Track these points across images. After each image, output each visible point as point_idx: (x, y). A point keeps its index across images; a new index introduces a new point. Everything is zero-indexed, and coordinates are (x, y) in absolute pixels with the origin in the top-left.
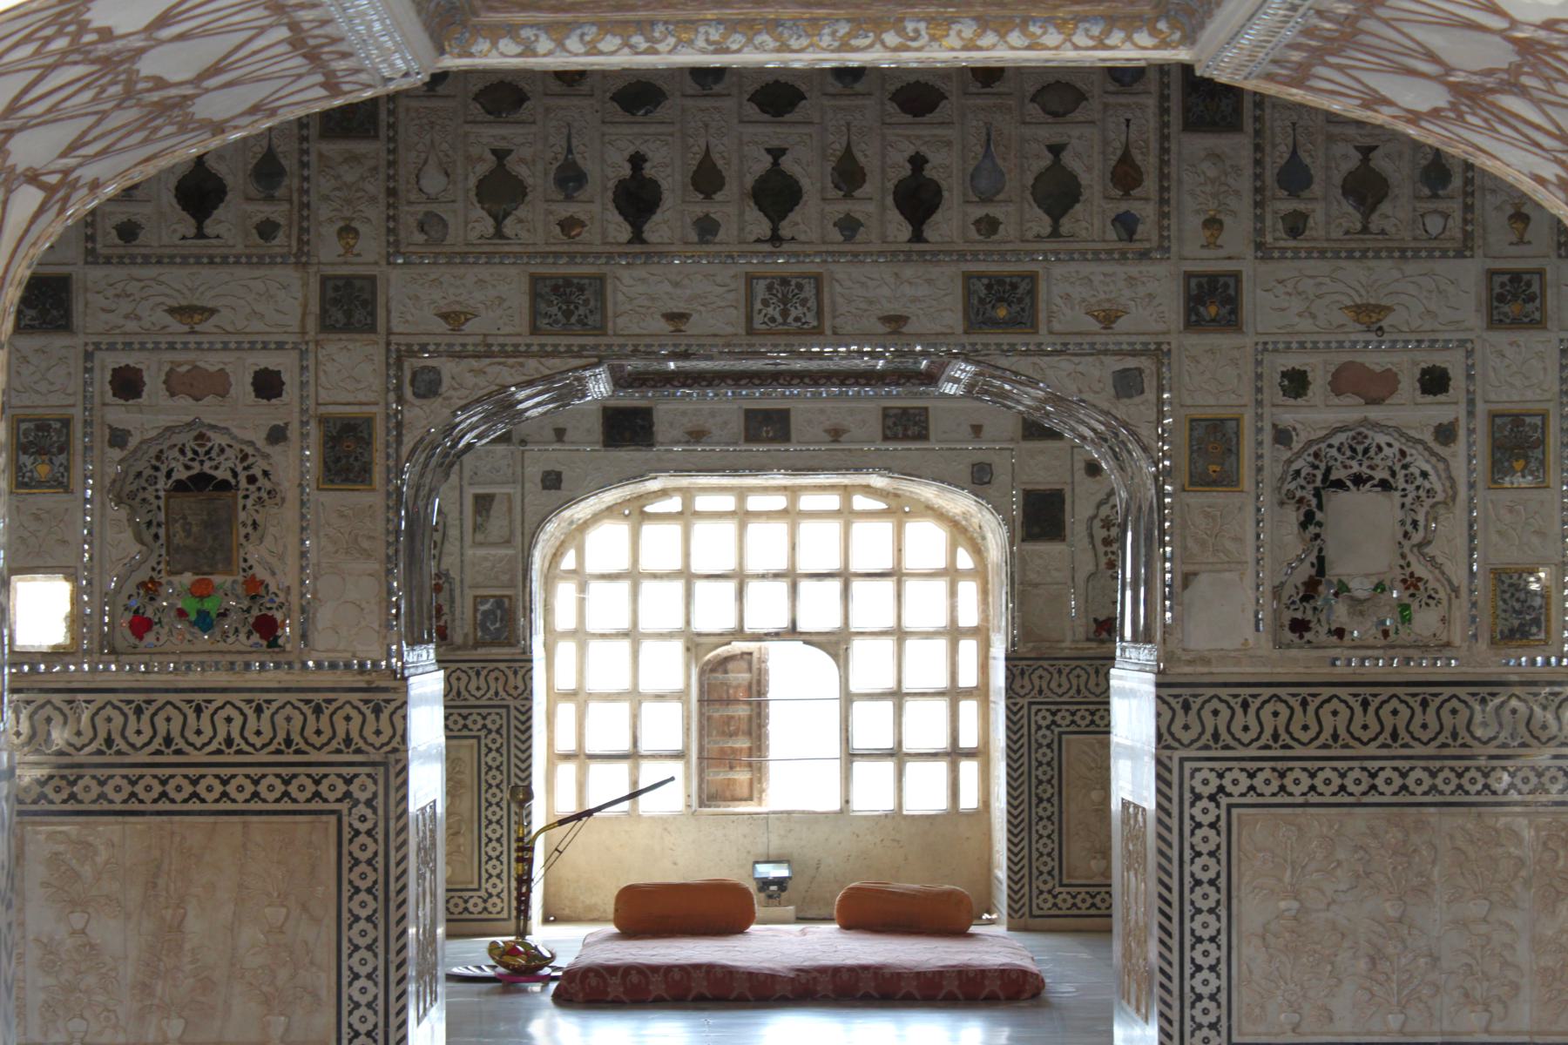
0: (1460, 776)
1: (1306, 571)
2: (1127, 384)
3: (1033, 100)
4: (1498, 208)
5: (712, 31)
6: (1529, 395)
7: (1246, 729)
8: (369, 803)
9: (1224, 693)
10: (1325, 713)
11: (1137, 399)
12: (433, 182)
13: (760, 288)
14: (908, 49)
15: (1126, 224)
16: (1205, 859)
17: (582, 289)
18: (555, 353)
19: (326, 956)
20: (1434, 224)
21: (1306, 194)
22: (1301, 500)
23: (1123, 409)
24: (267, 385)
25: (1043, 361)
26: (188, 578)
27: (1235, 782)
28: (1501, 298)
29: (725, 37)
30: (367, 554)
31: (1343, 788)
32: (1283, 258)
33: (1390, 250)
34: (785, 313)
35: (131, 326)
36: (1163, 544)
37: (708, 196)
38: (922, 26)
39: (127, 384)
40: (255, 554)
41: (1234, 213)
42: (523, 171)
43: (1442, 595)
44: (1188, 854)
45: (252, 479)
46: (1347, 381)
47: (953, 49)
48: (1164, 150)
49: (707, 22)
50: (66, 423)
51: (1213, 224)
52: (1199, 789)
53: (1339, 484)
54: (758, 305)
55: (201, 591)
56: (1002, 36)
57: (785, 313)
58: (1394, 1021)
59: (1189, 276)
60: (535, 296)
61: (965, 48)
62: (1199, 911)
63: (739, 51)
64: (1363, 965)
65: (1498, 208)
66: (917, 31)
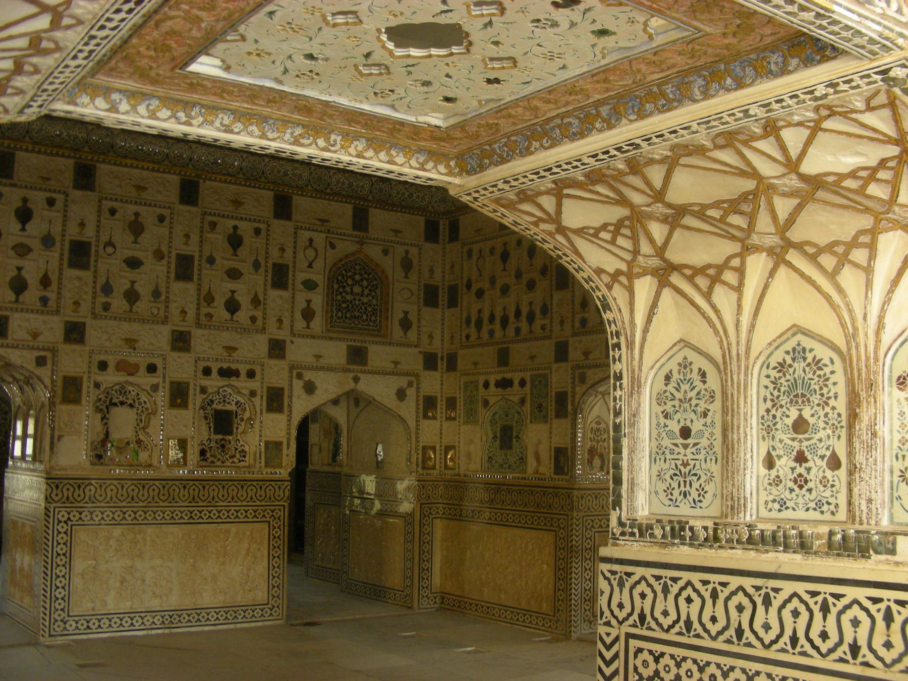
0: (155, 513)
1: (102, 436)
2: (41, 362)
3: (12, 248)
4: (177, 308)
5: (226, 118)
6: (184, 376)
7: (79, 496)
9: (71, 482)
10: (108, 491)
11: (45, 368)
14: (329, 151)
15: (44, 300)
16: (62, 546)
20: (155, 311)
21: (111, 296)
22: (101, 410)
23: (39, 371)
25: (9, 350)
27: (74, 516)
28: (176, 340)
29: (233, 123)
31: (113, 518)
32: (101, 318)
33: (139, 320)
36: (87, 426)
38: (339, 138)
41: (85, 300)
43: (149, 447)
44: (55, 544)
46: (122, 366)
47: (351, 155)
48: (61, 274)
49: (224, 110)
51: (77, 303)
52: (61, 518)
53: (115, 404)
56: (377, 153)
58: (129, 604)
59: (67, 322)
61: (358, 156)
62: (58, 566)
63: (238, 133)
64: (118, 584)
65: (177, 308)
66: (335, 141)
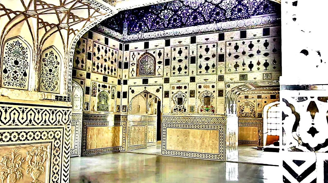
8: (222, 129)
12: (230, 66)
13: (264, 75)
17: (245, 76)
18: (242, 83)
19: (218, 144)
24: (213, 87)
26: (206, 106)
30: (223, 103)
34: (267, 77)
35: (200, 81)
37: (259, 65)
39: (200, 87)
40: (211, 103)
42: (239, 64)
45: (212, 96)
50: (194, 91)
54: (264, 77)
55: (207, 107)
57: (267, 77)
60: (240, 77)
